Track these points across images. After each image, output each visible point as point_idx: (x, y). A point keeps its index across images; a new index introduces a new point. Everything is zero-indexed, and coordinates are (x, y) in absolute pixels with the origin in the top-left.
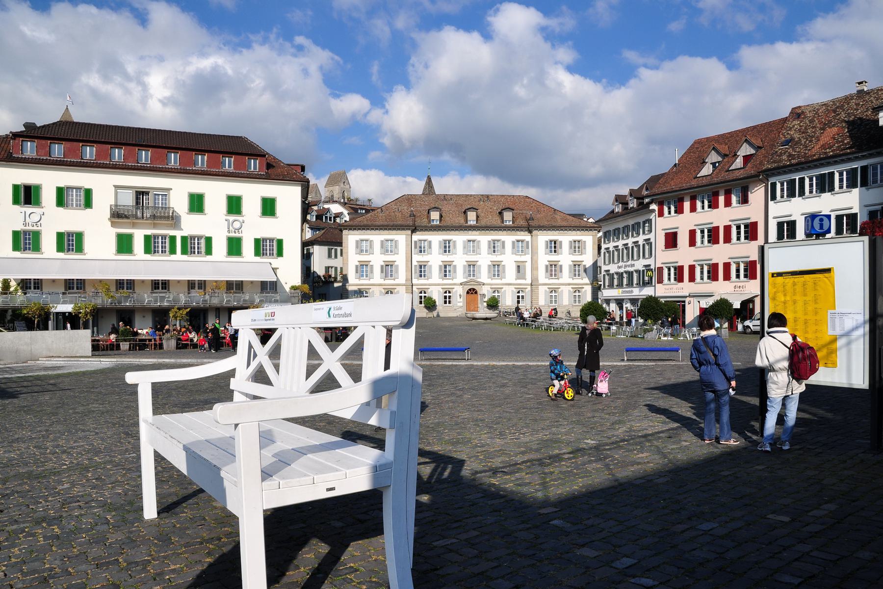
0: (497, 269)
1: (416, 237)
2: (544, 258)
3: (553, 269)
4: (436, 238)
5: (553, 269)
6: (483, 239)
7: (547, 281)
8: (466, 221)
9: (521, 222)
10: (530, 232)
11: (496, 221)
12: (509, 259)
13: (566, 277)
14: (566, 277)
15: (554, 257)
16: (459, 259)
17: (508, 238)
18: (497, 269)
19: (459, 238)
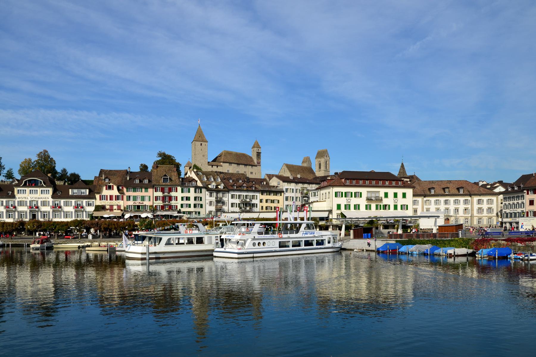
0: (457, 210)
1: (425, 199)
2: (476, 206)
3: (480, 210)
4: (433, 199)
5: (480, 210)
6: (452, 199)
7: (477, 215)
8: (445, 192)
9: (467, 193)
10: (471, 196)
11: (457, 192)
12: (461, 207)
13: (485, 213)
14: (485, 213)
15: (480, 206)
16: (442, 207)
17: (462, 199)
18: (457, 210)
19: (442, 199)
